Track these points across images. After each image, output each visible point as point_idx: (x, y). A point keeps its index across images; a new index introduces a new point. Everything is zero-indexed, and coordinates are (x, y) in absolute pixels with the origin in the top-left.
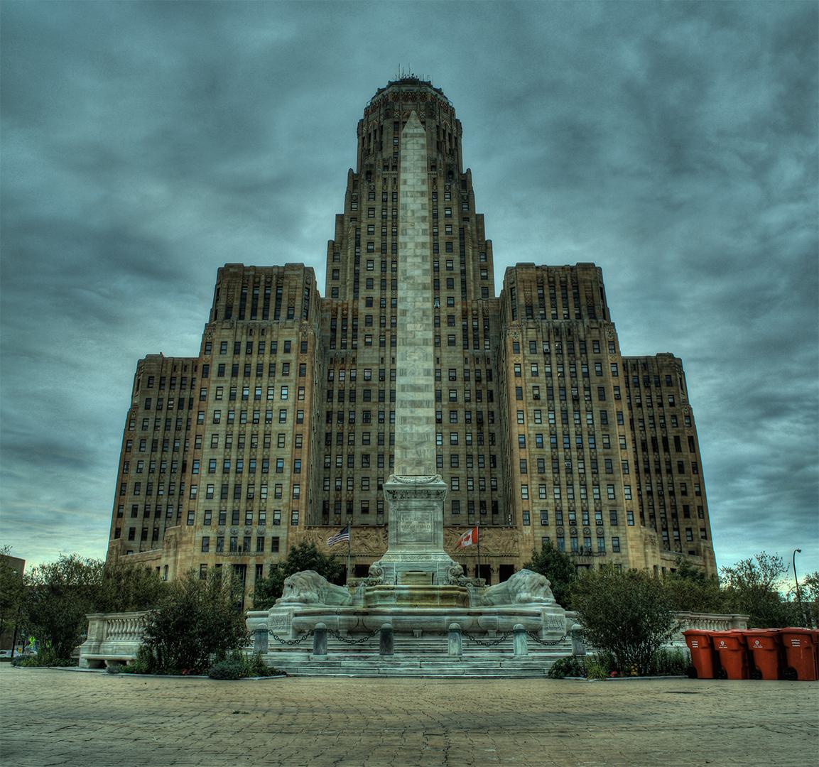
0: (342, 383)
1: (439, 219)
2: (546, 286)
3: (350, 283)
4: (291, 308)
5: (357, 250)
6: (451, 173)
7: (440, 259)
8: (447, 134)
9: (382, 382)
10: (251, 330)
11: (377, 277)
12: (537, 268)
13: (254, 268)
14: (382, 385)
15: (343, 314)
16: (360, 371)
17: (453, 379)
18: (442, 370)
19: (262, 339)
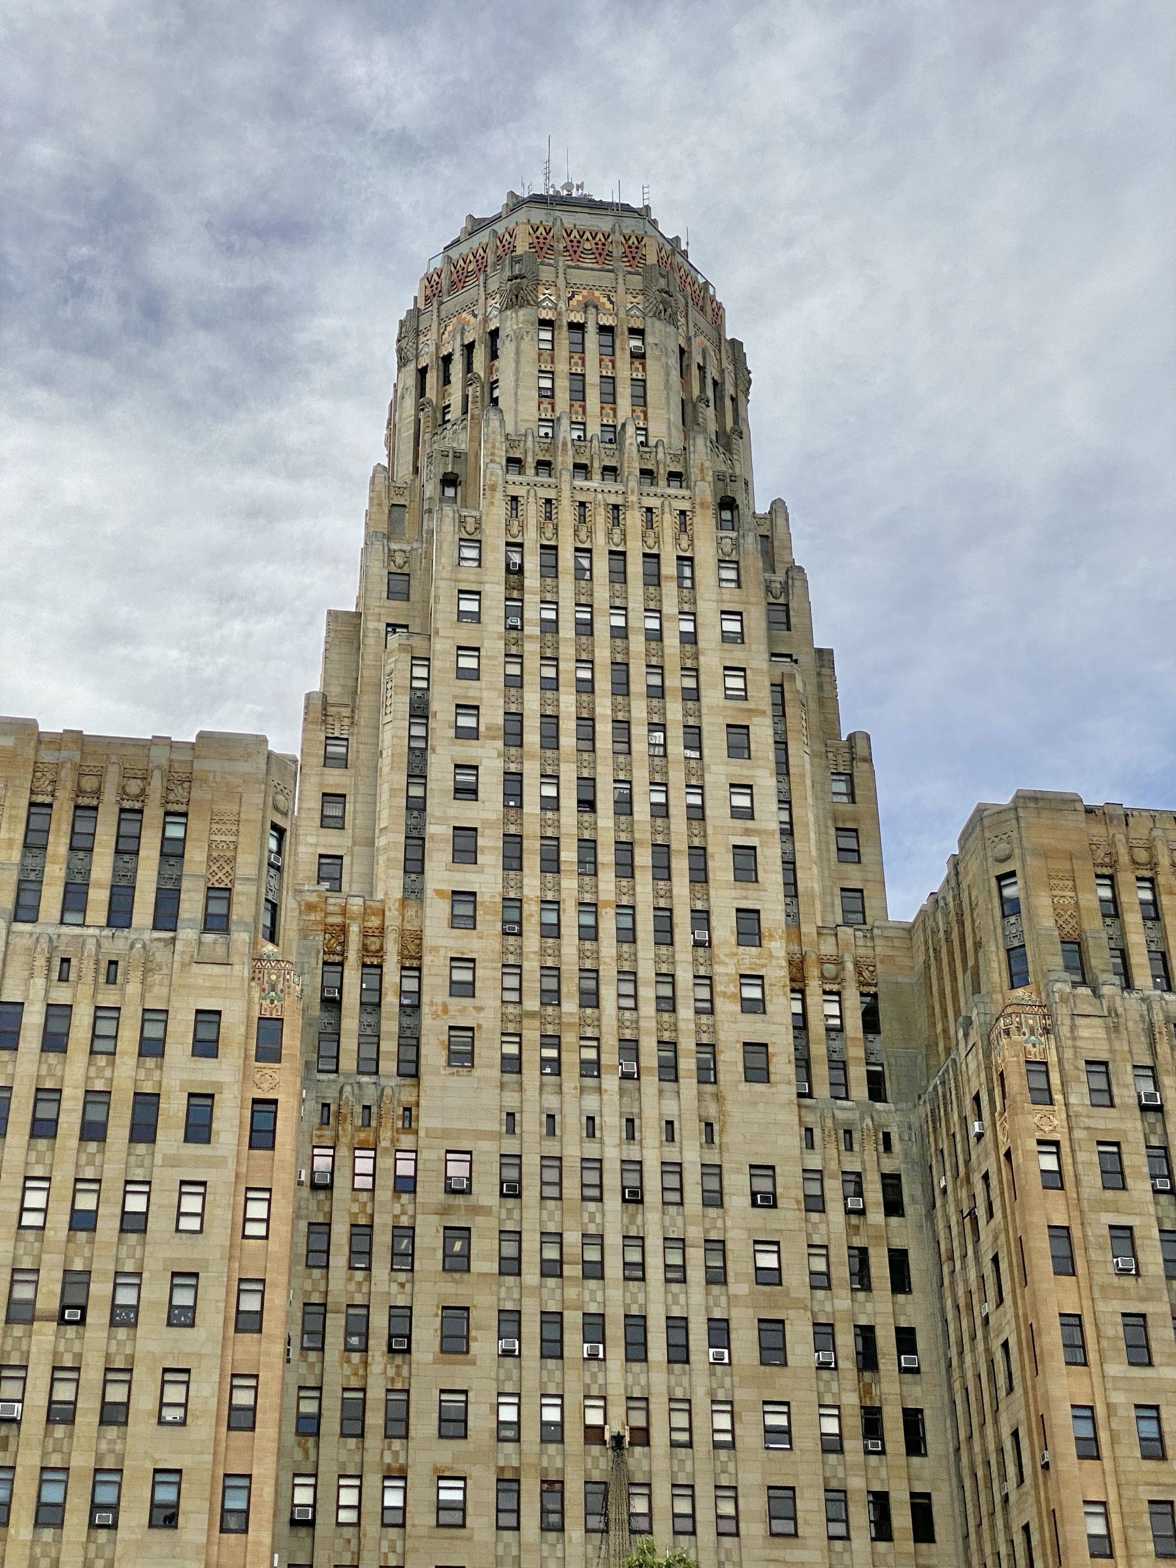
0: (364, 1197)
1: (702, 644)
2: (1126, 878)
3: (391, 841)
4: (219, 893)
5: (418, 731)
6: (727, 504)
7: (707, 777)
8: (709, 382)
9: (511, 1203)
10: (66, 961)
11: (487, 823)
12: (1089, 811)
13: (78, 738)
14: (509, 1211)
15: (365, 948)
16: (431, 1155)
17: (765, 1201)
18: (725, 1166)
19: (109, 998)
